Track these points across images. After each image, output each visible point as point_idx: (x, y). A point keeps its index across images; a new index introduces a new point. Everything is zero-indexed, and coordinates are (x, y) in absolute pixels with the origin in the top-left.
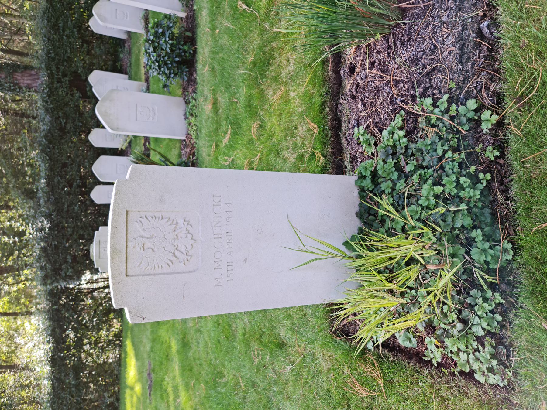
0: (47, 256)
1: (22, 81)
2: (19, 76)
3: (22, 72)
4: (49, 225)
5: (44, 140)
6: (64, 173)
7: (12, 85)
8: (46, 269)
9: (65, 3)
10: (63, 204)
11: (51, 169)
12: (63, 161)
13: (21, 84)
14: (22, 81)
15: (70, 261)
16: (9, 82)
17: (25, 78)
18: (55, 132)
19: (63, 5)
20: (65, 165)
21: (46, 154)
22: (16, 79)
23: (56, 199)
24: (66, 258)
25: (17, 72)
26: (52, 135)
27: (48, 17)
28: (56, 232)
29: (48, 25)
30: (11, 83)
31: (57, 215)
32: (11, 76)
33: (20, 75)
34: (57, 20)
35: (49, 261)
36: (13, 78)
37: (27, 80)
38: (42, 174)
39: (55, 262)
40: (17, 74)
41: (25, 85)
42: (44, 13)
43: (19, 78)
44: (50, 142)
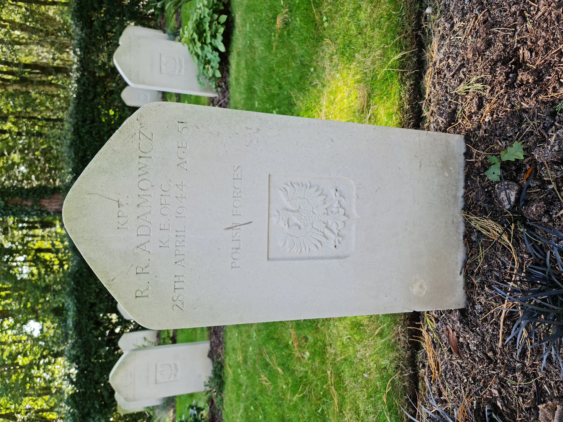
0: (75, 402)
1: (50, 207)
2: (46, 203)
3: (50, 198)
4: (76, 371)
5: (72, 283)
6: (92, 313)
7: (39, 212)
8: (74, 415)
9: (94, 133)
10: (91, 348)
11: (79, 312)
12: (91, 301)
13: (49, 210)
14: (50, 207)
15: (98, 407)
16: (36, 210)
17: (54, 204)
18: (84, 272)
19: (92, 135)
20: (93, 305)
21: (76, 296)
22: (44, 206)
23: (83, 343)
24: (94, 404)
25: (43, 198)
26: (80, 275)
27: (75, 150)
28: (84, 380)
29: (75, 158)
30: (39, 210)
31: (85, 359)
32: (38, 203)
33: (47, 201)
34: (85, 151)
35: (77, 407)
36: (40, 205)
37: (55, 206)
38: (71, 313)
39: (83, 409)
40: (44, 201)
41: (54, 210)
42: (72, 144)
43: (46, 205)
44: (77, 283)
